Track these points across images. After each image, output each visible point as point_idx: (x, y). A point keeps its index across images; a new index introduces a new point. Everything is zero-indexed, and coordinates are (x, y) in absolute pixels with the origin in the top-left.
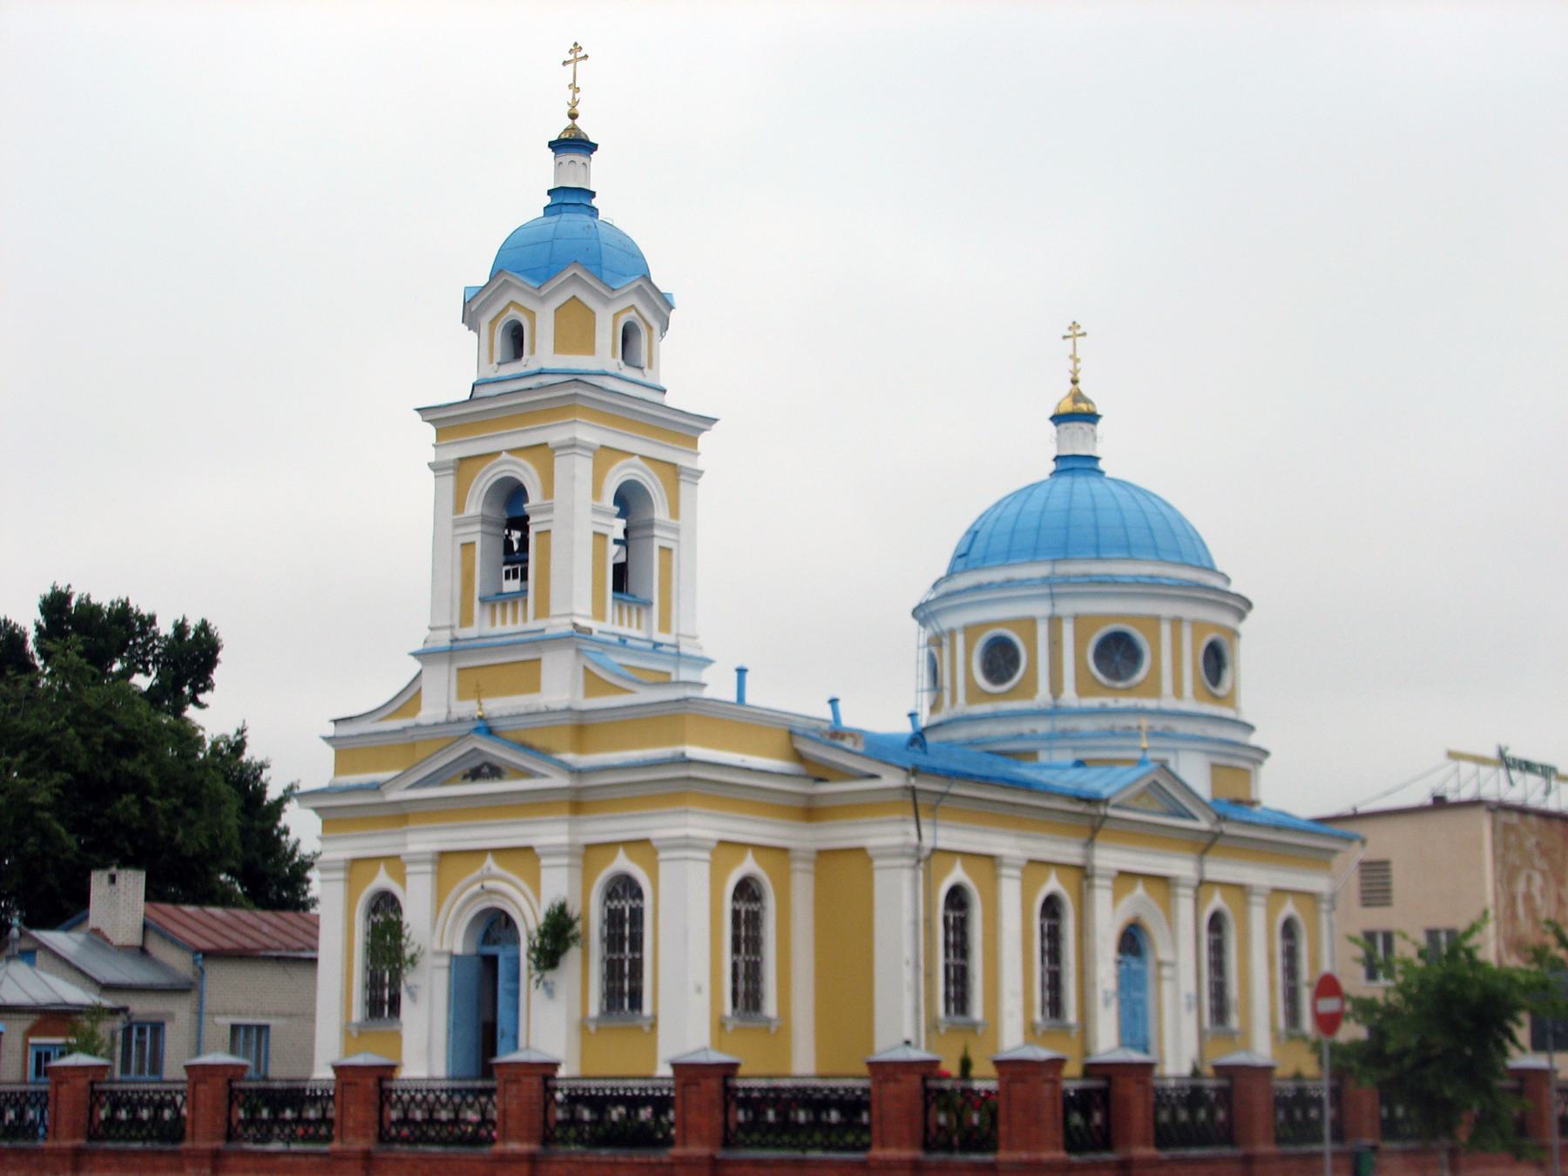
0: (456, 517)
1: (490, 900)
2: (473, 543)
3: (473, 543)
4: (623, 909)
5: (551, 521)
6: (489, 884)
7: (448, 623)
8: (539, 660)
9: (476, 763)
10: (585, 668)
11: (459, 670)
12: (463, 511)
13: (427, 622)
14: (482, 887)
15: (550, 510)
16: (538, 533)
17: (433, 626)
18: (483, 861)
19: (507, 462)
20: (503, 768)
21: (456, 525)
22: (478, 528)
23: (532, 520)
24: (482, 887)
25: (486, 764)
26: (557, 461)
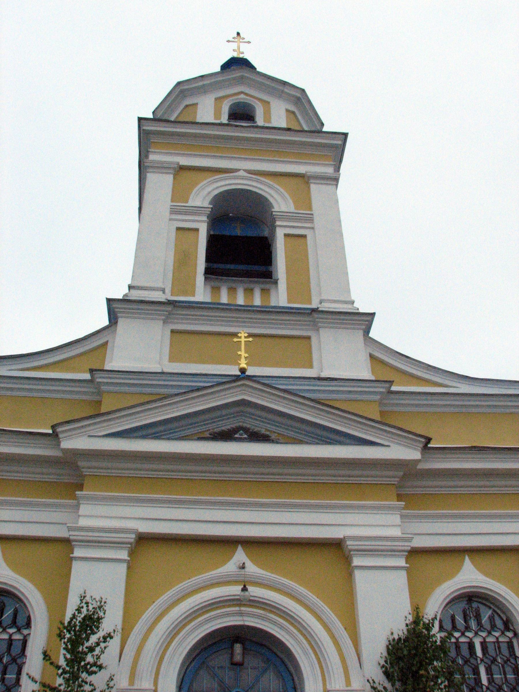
0: (172, 204)
1: (241, 614)
2: (197, 230)
3: (197, 230)
4: (471, 646)
5: (313, 228)
6: (254, 591)
7: (160, 285)
8: (309, 338)
9: (226, 425)
10: (371, 356)
11: (173, 331)
12: (187, 202)
13: (129, 282)
14: (244, 589)
15: (310, 219)
16: (286, 235)
17: (135, 284)
18: (234, 552)
19: (243, 178)
20: (273, 436)
21: (171, 214)
22: (205, 218)
23: (278, 223)
24: (244, 589)
25: (246, 430)
26: (313, 187)
